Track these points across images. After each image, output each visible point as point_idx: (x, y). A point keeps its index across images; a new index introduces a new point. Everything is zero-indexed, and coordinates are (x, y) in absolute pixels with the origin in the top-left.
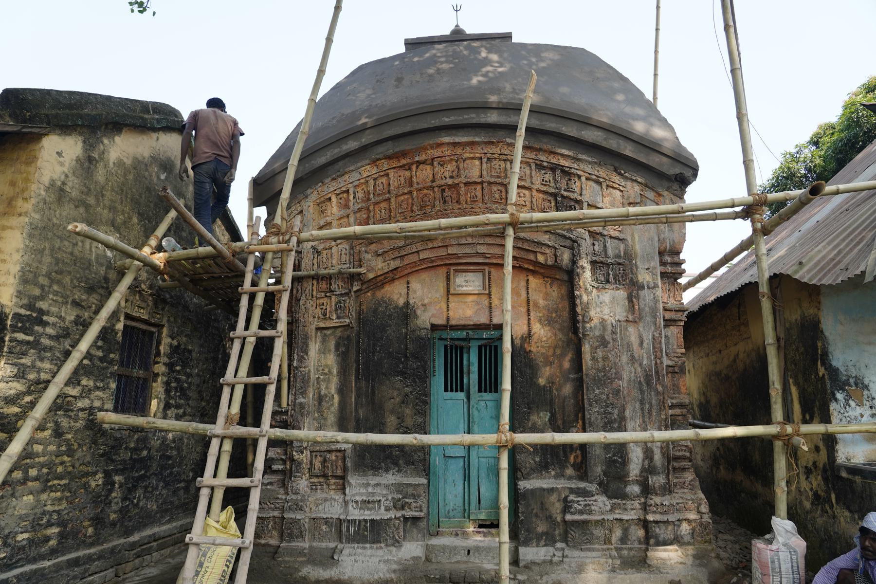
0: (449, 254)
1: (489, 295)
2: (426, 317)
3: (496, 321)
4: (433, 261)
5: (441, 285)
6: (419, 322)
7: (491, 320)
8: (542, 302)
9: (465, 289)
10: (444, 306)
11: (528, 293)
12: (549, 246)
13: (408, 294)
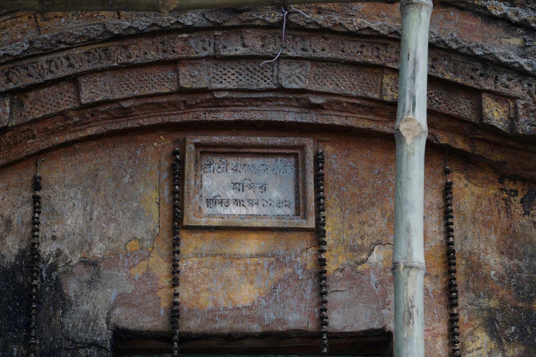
0: (182, 91)
1: (318, 234)
2: (99, 305)
3: (339, 321)
4: (126, 113)
5: (151, 196)
6: (73, 322)
7: (322, 320)
8: (494, 262)
9: (234, 212)
10: (162, 269)
11: (448, 231)
12: (521, 73)
13: (35, 222)
